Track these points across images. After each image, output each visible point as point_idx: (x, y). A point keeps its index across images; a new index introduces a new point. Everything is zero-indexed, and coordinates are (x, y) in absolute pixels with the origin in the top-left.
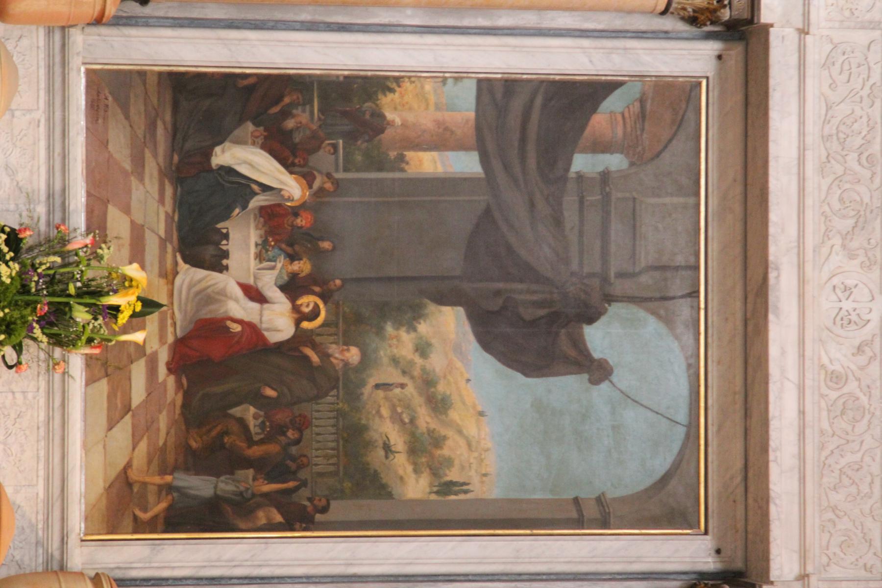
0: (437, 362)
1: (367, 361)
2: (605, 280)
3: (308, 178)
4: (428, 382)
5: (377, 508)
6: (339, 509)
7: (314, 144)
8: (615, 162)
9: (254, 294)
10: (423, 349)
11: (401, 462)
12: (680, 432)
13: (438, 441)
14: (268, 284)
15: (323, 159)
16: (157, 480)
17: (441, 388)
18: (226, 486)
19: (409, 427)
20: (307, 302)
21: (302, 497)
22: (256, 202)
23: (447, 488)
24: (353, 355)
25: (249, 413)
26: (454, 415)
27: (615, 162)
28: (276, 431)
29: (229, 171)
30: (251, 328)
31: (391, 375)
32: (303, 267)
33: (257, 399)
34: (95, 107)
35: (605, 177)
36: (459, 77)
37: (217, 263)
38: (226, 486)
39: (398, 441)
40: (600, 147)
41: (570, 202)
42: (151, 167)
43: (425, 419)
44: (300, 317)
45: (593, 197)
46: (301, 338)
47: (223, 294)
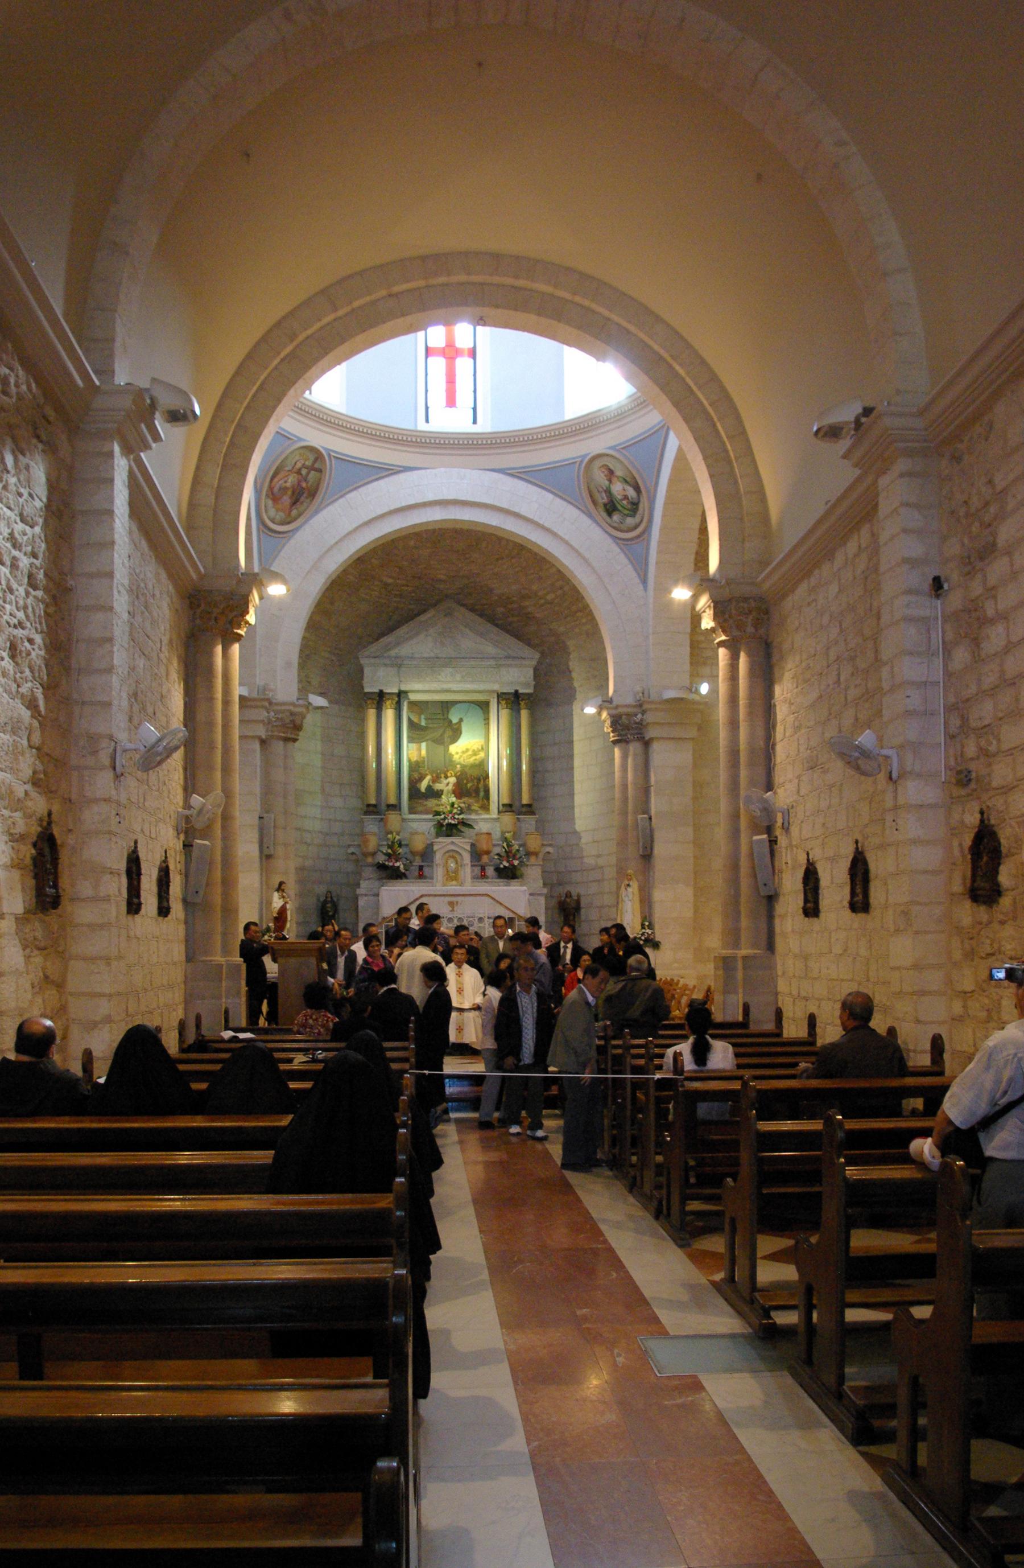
0: (460, 751)
1: (459, 763)
2: (444, 719)
3: (426, 775)
4: (463, 752)
5: (485, 762)
6: (486, 769)
7: (420, 773)
8: (423, 717)
9: (448, 784)
10: (457, 753)
11: (478, 757)
12: (473, 705)
13: (474, 750)
14: (445, 782)
15: (423, 772)
16: (481, 802)
17: (464, 749)
18: (482, 790)
19: (472, 756)
20: (449, 775)
21: (484, 775)
22: (431, 784)
23: (482, 748)
24: (458, 766)
25: (469, 785)
26: (469, 747)
27: (423, 717)
28: (472, 780)
29: (426, 790)
30: (454, 785)
31: (462, 759)
32: (443, 776)
33: (466, 784)
34: (415, 813)
35: (426, 719)
36: (408, 746)
37: (442, 791)
38: (482, 790)
39: (474, 758)
40: (420, 719)
41: (431, 726)
42: (425, 803)
43: (470, 753)
44: (452, 776)
45: (430, 721)
46: (455, 776)
47: (448, 792)
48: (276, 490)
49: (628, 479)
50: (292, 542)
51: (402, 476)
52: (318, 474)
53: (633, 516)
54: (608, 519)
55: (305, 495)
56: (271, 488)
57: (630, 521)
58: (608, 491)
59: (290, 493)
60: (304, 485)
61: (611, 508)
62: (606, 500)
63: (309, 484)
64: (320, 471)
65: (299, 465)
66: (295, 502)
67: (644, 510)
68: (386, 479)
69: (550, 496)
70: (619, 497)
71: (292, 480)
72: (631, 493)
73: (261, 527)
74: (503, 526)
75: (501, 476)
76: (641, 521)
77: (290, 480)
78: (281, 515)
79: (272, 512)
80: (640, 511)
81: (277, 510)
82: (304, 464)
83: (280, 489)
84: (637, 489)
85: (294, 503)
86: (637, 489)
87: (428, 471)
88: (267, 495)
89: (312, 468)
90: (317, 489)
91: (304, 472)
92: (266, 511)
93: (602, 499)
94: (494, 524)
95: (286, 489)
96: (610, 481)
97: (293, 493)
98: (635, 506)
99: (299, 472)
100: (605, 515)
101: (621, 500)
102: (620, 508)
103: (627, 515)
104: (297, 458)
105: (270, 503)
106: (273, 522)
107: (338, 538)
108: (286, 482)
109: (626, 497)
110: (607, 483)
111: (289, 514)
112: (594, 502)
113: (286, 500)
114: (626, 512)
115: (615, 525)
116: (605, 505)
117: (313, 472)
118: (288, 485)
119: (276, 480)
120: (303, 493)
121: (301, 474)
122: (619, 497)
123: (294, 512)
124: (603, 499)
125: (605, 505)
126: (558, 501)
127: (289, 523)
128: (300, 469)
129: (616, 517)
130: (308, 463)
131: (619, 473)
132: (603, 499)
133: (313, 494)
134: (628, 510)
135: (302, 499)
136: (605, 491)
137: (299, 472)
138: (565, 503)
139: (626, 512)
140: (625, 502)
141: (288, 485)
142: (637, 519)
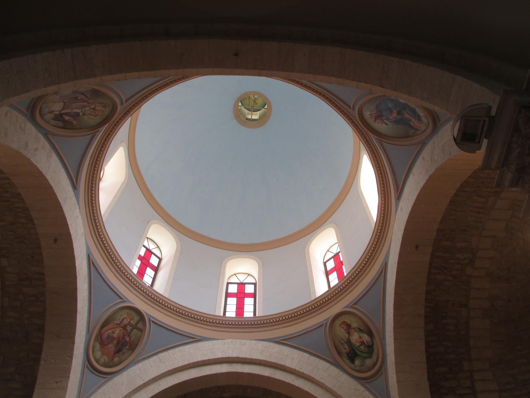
48: (105, 336)
49: (362, 328)
50: (110, 383)
51: (200, 344)
52: (139, 333)
53: (370, 357)
54: (352, 365)
55: (127, 347)
56: (100, 334)
57: (369, 362)
58: (349, 342)
59: (115, 342)
60: (127, 339)
61: (352, 356)
62: (348, 350)
63: (131, 339)
64: (142, 331)
65: (126, 322)
66: (119, 351)
67: (378, 348)
68: (189, 346)
69: (307, 355)
70: (358, 344)
71: (118, 332)
72: (366, 338)
73: (86, 362)
74: (272, 376)
75: (271, 344)
76: (378, 359)
77: (117, 332)
78: (104, 359)
79: (98, 354)
80: (375, 352)
81: (103, 354)
82: (129, 322)
83: (108, 337)
84: (370, 334)
85: (118, 352)
86: (370, 334)
87: (220, 341)
88: (96, 339)
89: (135, 327)
90: (137, 345)
91: (129, 328)
92: (93, 351)
93: (345, 349)
94: (266, 375)
95: (113, 338)
96: (349, 333)
97: (118, 343)
98: (370, 348)
99: (125, 327)
100: (348, 362)
101: (360, 346)
102: (359, 353)
103: (365, 358)
104: (125, 316)
105: (98, 346)
106: (97, 361)
107: (146, 380)
108: (113, 333)
109: (363, 343)
110: (347, 335)
111: (113, 359)
112: (340, 353)
113: (112, 347)
114: (364, 355)
115: (357, 368)
116: (348, 354)
117: (135, 330)
118: (115, 335)
119: (105, 328)
120: (126, 346)
121: (126, 330)
122: (358, 344)
123: (116, 359)
124: (345, 349)
125: (348, 354)
126: (313, 358)
127: (110, 367)
128: (126, 326)
129: (357, 362)
130: (133, 322)
131: (354, 325)
132: (345, 349)
133: (133, 347)
134: (365, 353)
135: (124, 350)
136: (346, 343)
137: (125, 327)
138: (318, 360)
139: (364, 355)
140: (362, 347)
141: (115, 335)
142: (374, 357)
